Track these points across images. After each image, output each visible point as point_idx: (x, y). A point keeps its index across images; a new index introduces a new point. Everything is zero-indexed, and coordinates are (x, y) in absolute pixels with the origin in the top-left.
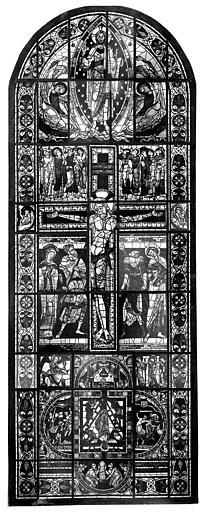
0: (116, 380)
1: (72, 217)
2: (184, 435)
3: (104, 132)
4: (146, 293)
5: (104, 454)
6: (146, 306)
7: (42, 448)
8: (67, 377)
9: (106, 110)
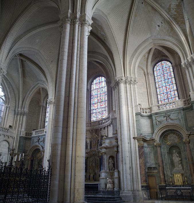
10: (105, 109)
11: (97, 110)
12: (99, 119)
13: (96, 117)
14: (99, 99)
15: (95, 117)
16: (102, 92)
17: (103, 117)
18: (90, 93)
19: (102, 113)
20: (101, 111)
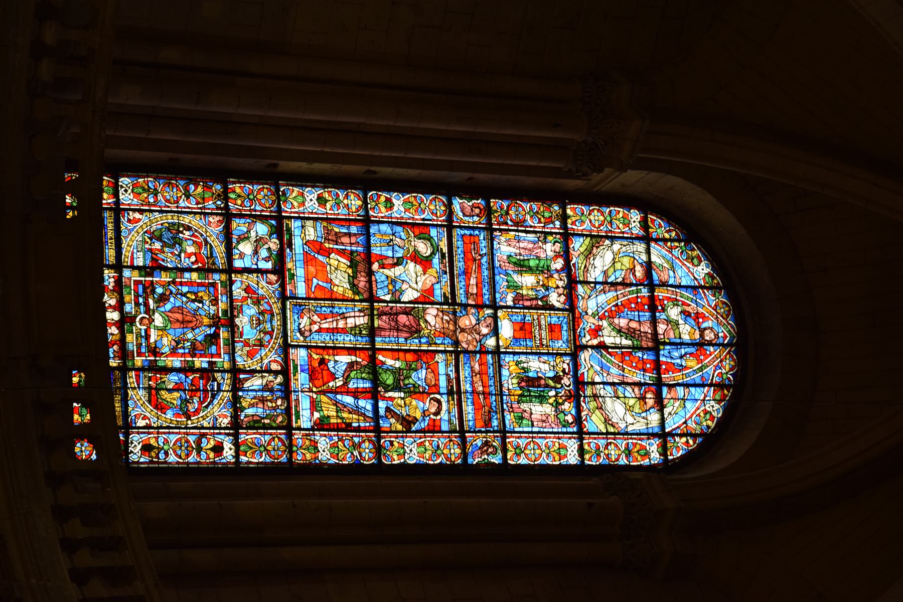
0: (246, 344)
1: (473, 281)
2: (166, 454)
3: (588, 337)
4: (374, 395)
5: (132, 320)
6: (356, 394)
7: (137, 215)
8: (248, 263)
9: (618, 340)
10: (256, 424)
11: (266, 287)
12: (126, 321)
13: (154, 267)
14: (415, 331)
15: (169, 259)
16: (510, 383)
17: (137, 396)
18: (529, 181)
19: (208, 373)
20: (240, 361)
